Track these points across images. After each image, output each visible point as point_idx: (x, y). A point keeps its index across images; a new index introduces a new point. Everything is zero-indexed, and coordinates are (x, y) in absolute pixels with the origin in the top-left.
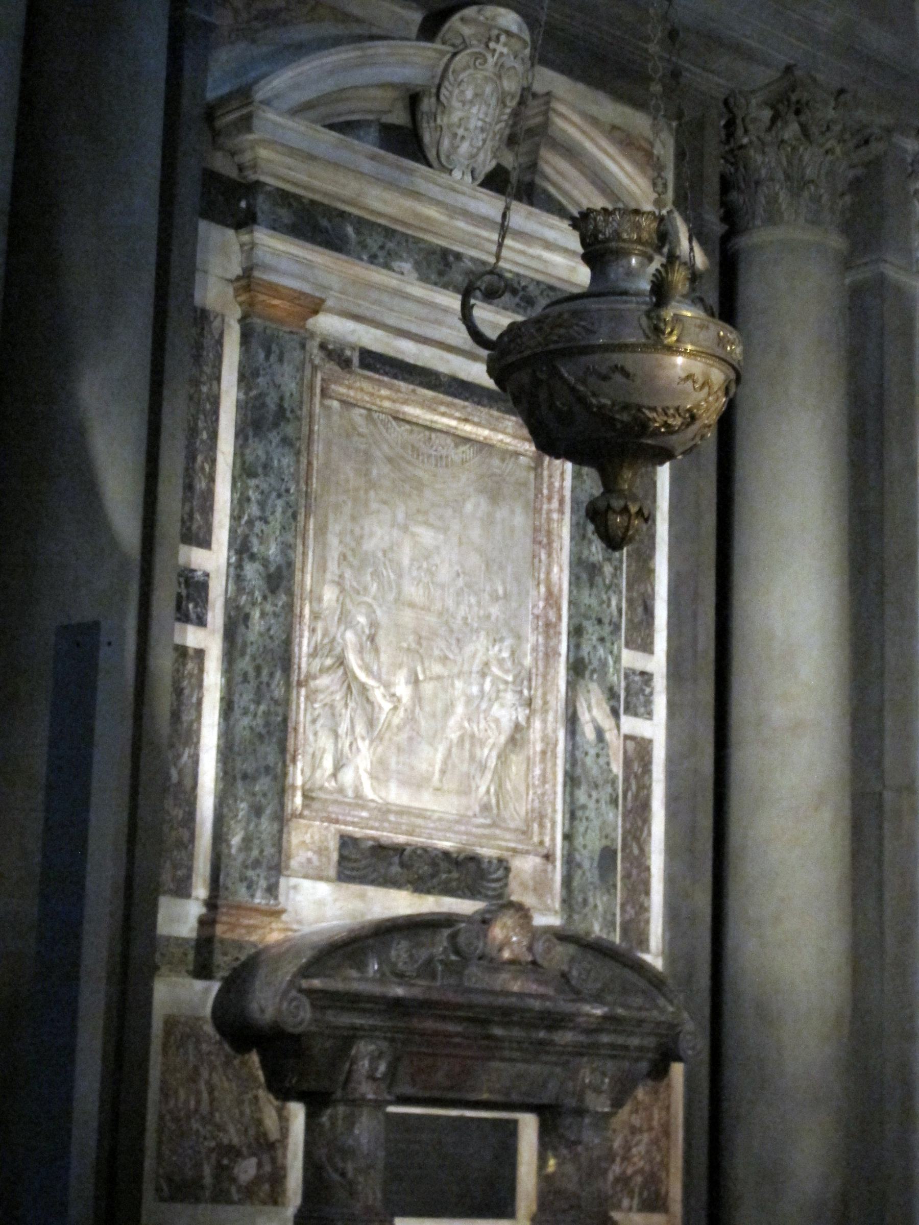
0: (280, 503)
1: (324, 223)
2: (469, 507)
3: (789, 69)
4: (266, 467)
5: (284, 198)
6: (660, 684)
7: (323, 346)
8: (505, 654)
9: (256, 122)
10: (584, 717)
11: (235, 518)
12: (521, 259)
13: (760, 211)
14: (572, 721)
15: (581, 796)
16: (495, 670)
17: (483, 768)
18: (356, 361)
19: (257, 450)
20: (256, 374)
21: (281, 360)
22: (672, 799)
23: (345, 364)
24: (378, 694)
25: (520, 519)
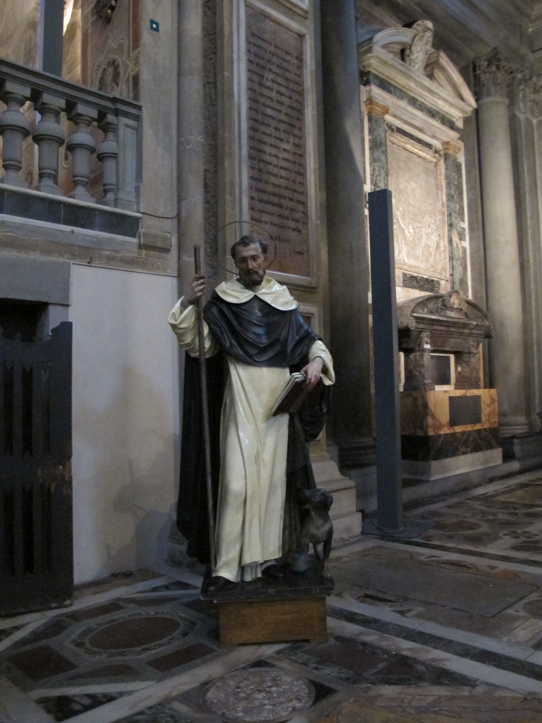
0: (383, 171)
1: (386, 85)
2: (422, 177)
3: (495, 48)
4: (379, 159)
5: (376, 77)
6: (467, 231)
7: (387, 124)
8: (433, 221)
9: (373, 49)
10: (454, 240)
11: (372, 175)
12: (432, 102)
13: (485, 93)
14: (450, 241)
15: (454, 262)
16: (432, 226)
17: (431, 254)
18: (395, 130)
19: (376, 154)
20: (374, 130)
21: (380, 127)
22: (472, 265)
23: (392, 130)
24: (406, 231)
25: (433, 181)
